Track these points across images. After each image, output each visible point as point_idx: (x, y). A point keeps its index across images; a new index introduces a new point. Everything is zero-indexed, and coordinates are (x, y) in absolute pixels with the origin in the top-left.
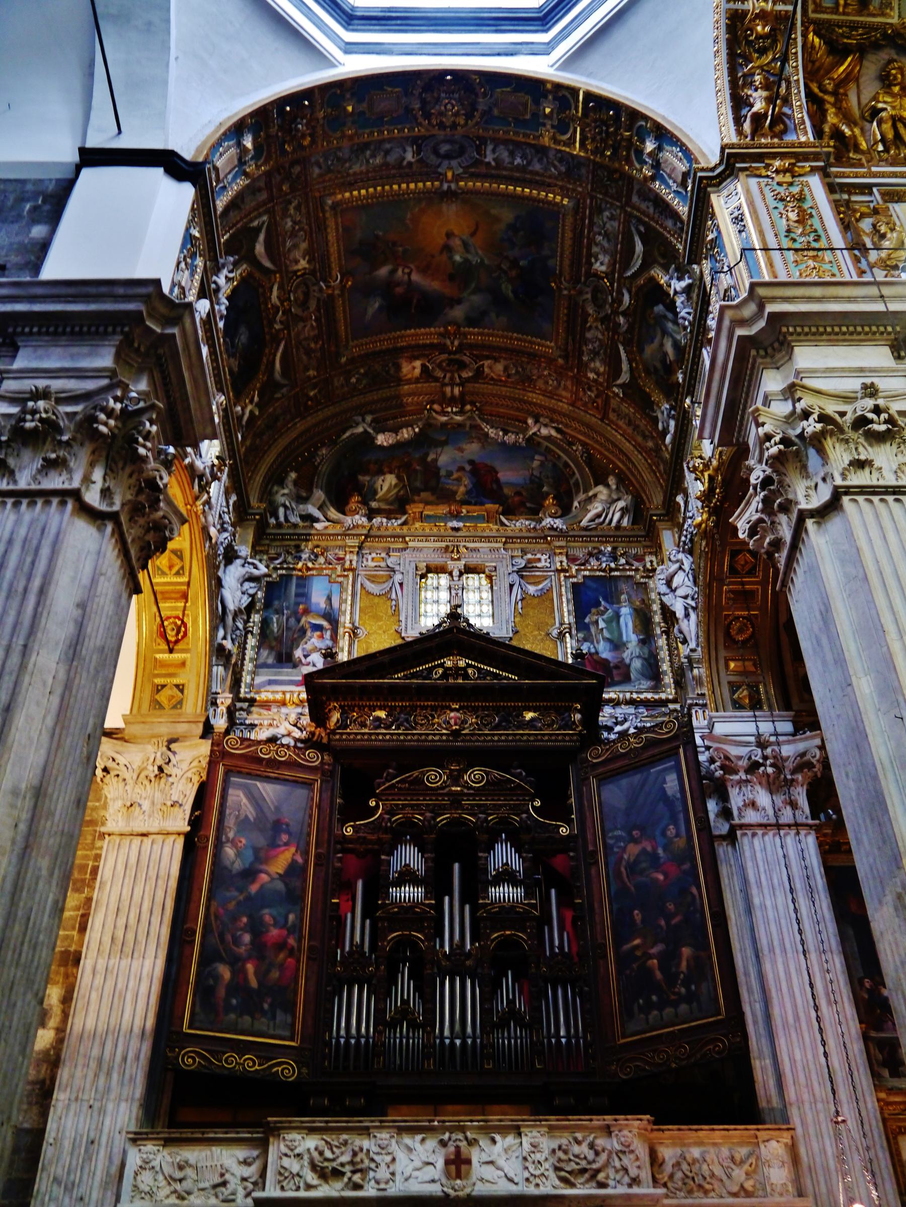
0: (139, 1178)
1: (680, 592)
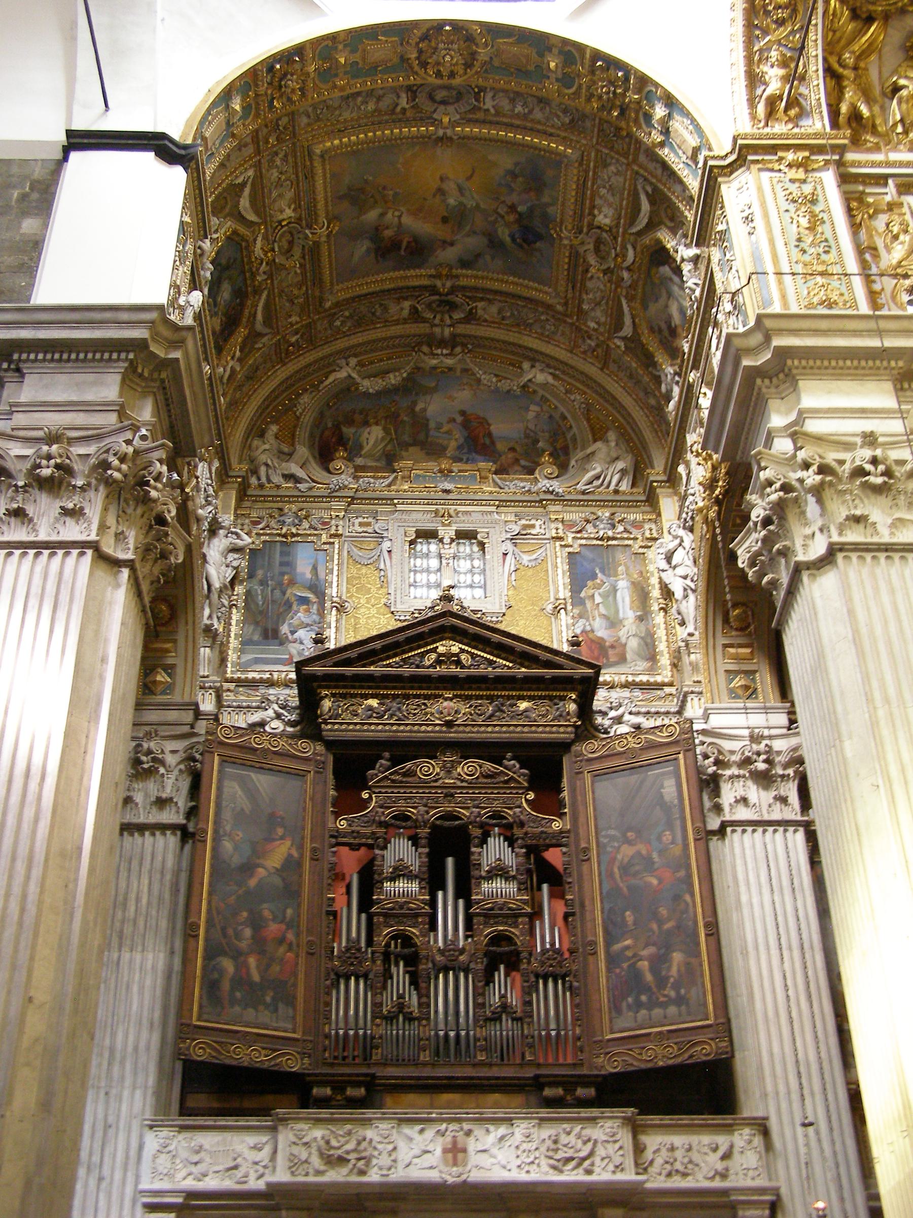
1: (680, 571)
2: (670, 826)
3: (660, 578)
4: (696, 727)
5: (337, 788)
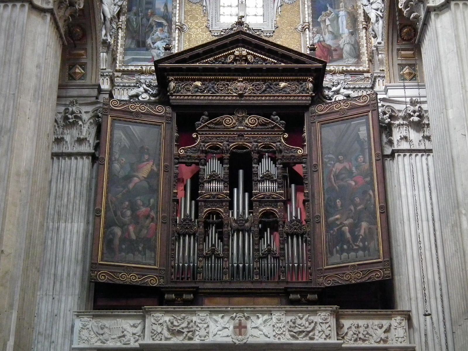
0: (81, 333)
1: (375, 6)
2: (362, 152)
3: (364, 10)
4: (379, 97)
5: (179, 131)
